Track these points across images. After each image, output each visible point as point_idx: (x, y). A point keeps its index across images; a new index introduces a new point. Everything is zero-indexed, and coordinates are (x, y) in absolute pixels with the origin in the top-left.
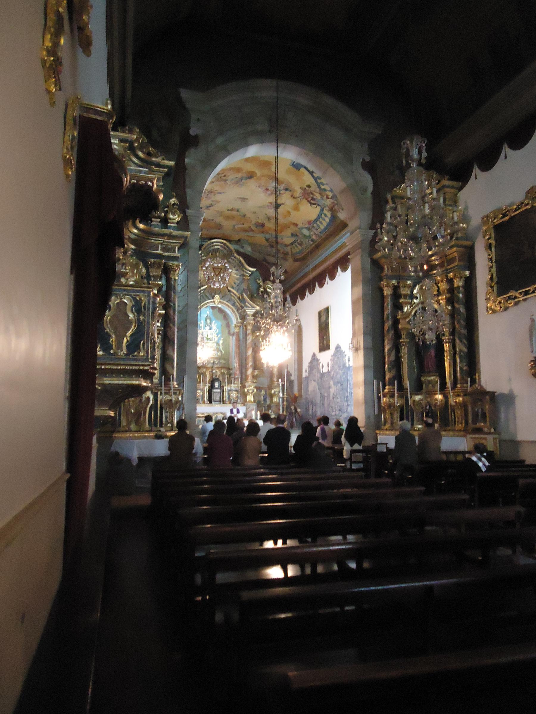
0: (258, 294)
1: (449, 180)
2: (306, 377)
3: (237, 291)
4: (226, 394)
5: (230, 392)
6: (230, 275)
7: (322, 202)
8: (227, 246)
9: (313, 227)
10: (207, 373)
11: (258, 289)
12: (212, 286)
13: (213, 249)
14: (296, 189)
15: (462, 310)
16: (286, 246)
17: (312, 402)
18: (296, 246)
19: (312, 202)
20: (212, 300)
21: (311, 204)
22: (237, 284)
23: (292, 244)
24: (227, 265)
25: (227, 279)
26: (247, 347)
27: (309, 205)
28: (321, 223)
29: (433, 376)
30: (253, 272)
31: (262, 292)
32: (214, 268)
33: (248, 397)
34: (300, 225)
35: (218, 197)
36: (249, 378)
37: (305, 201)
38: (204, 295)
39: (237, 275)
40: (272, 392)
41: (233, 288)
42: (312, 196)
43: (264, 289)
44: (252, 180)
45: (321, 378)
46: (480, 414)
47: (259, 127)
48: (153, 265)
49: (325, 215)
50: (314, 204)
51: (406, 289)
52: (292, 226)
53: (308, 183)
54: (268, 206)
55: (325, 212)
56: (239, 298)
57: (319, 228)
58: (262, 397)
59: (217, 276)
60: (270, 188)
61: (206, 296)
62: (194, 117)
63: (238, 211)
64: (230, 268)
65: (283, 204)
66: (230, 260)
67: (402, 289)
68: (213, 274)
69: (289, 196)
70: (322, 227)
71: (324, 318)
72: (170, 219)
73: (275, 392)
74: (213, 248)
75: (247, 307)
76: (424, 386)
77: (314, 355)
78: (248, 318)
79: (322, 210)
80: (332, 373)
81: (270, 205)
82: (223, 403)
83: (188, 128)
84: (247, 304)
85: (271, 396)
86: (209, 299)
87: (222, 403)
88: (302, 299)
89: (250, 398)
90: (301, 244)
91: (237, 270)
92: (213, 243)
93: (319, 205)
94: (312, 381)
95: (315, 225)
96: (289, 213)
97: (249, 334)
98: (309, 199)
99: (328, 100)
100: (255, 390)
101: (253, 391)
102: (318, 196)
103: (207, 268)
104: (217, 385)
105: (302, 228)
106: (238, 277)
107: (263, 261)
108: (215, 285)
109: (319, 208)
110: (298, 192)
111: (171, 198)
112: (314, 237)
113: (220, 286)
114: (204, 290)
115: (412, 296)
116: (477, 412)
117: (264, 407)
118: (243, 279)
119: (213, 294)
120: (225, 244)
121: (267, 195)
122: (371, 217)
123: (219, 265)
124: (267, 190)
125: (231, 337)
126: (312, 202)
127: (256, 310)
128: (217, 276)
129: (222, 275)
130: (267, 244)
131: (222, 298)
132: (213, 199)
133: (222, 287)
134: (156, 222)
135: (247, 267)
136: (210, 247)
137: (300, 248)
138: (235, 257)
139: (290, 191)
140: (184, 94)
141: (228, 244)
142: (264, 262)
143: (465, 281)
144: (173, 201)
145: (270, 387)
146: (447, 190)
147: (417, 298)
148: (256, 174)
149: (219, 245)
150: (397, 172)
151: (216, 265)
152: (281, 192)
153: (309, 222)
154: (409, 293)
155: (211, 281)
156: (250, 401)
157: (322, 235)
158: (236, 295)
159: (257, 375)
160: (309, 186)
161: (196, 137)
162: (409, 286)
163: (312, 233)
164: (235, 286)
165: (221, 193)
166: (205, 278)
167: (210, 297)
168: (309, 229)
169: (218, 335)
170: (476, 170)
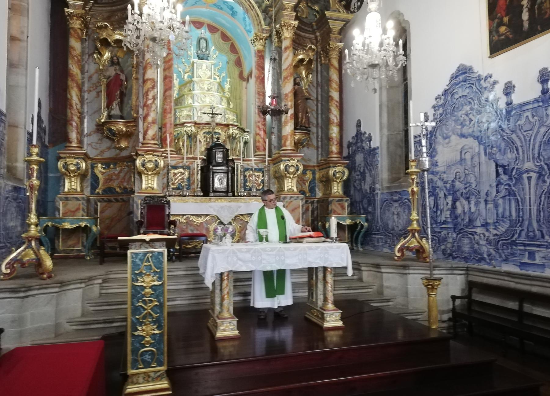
4: (240, 178)
5: (247, 174)
10: (200, 136)
17: (452, 191)
26: (284, 74)
33: (286, 181)
36: (288, 143)
58: (307, 184)
73: (334, 175)
78: (285, 12)
82: (234, 196)
85: (327, 182)
87: (230, 194)
89: (290, 184)
94: (454, 138)
97: (286, 48)
100: (301, 168)
101: (298, 170)
104: (219, 157)
117: (312, 203)
125: (244, 83)
159: (299, 140)
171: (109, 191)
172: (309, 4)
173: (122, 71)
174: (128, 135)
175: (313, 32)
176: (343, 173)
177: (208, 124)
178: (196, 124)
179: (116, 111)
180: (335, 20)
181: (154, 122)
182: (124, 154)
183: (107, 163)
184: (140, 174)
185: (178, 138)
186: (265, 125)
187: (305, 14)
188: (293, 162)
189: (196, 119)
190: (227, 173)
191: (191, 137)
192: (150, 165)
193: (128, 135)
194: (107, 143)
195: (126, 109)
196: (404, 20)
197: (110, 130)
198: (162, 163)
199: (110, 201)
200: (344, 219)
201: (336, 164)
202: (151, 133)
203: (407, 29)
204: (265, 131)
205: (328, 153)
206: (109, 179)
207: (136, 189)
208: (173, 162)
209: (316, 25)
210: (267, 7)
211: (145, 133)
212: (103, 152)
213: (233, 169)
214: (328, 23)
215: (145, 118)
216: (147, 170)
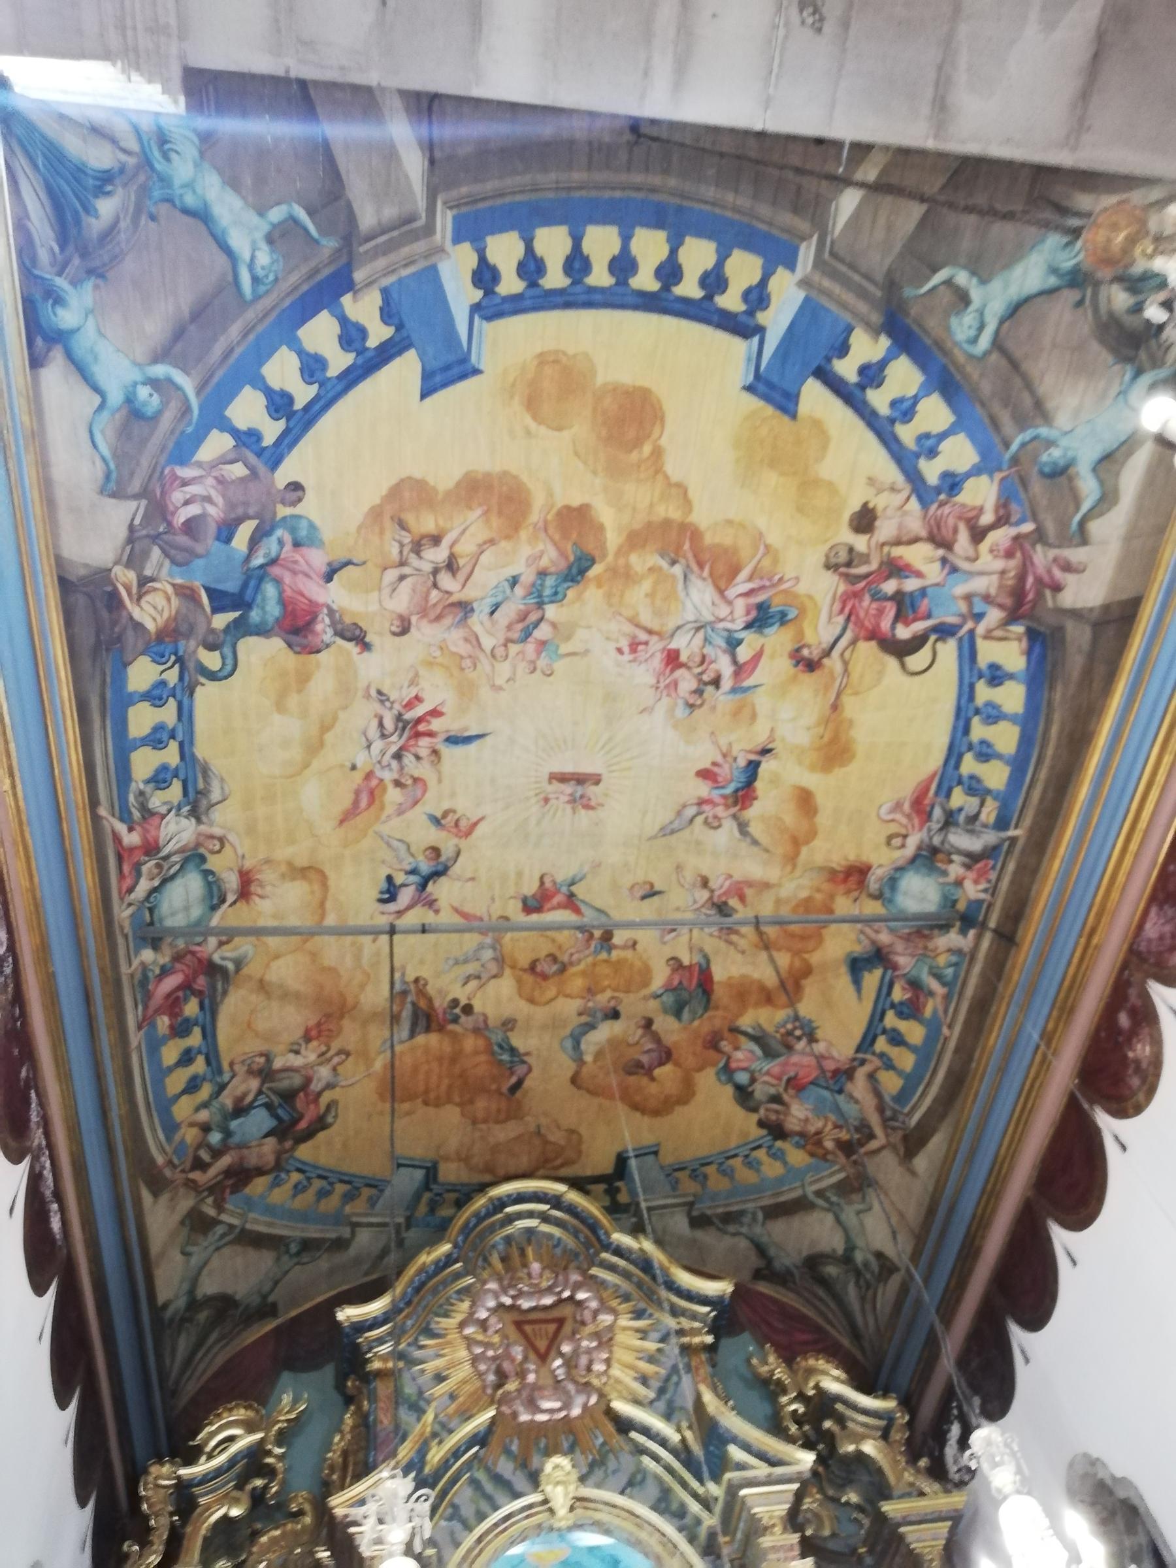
3: (668, 1416)
8: (571, 1210)
13: (508, 1240)
21: (901, 650)
22: (656, 1384)
24: (581, 1296)
31: (796, 1418)
32: (522, 1322)
34: (882, 860)
35: (459, 781)
37: (867, 649)
38: (481, 1475)
39: (643, 1334)
42: (890, 587)
43: (801, 1397)
50: (917, 643)
55: (988, 653)
59: (543, 1358)
61: (498, 1480)
63: (571, 902)
64: (604, 1307)
65: (766, 751)
66: (594, 1271)
68: (518, 1352)
74: (509, 1230)
78: (766, 1541)
81: (703, 789)
84: (736, 1453)
86: (517, 1495)
91: (638, 1314)
92: (500, 1204)
93: (944, 631)
96: (805, 801)
106: (651, 1346)
107: (758, 1275)
108: (533, 1406)
113: (567, 1406)
114: (481, 1439)
118: (685, 1349)
119: (535, 1461)
120: (556, 1202)
121: (681, 712)
123: (548, 1301)
124: (673, 659)
129: (566, 1348)
131: (593, 1468)
132: (433, 803)
133: (576, 1411)
135: (686, 1279)
136: (492, 1229)
137: (914, 1032)
138: (619, 1251)
141: (574, 1197)
142: (763, 1288)
149: (530, 1214)
151: (526, 1304)
152: (744, 654)
155: (511, 1386)
157: (1012, 833)
158: (663, 1442)
160: (864, 521)
165: (468, 740)
166: (480, 1375)
168: (930, 857)
172: (831, 1492)
180: (920, 1522)
187: (827, 1523)
196: (1113, 1478)
203: (1136, 1502)
209: (870, 1552)
210: (712, 1536)
214: (901, 1538)
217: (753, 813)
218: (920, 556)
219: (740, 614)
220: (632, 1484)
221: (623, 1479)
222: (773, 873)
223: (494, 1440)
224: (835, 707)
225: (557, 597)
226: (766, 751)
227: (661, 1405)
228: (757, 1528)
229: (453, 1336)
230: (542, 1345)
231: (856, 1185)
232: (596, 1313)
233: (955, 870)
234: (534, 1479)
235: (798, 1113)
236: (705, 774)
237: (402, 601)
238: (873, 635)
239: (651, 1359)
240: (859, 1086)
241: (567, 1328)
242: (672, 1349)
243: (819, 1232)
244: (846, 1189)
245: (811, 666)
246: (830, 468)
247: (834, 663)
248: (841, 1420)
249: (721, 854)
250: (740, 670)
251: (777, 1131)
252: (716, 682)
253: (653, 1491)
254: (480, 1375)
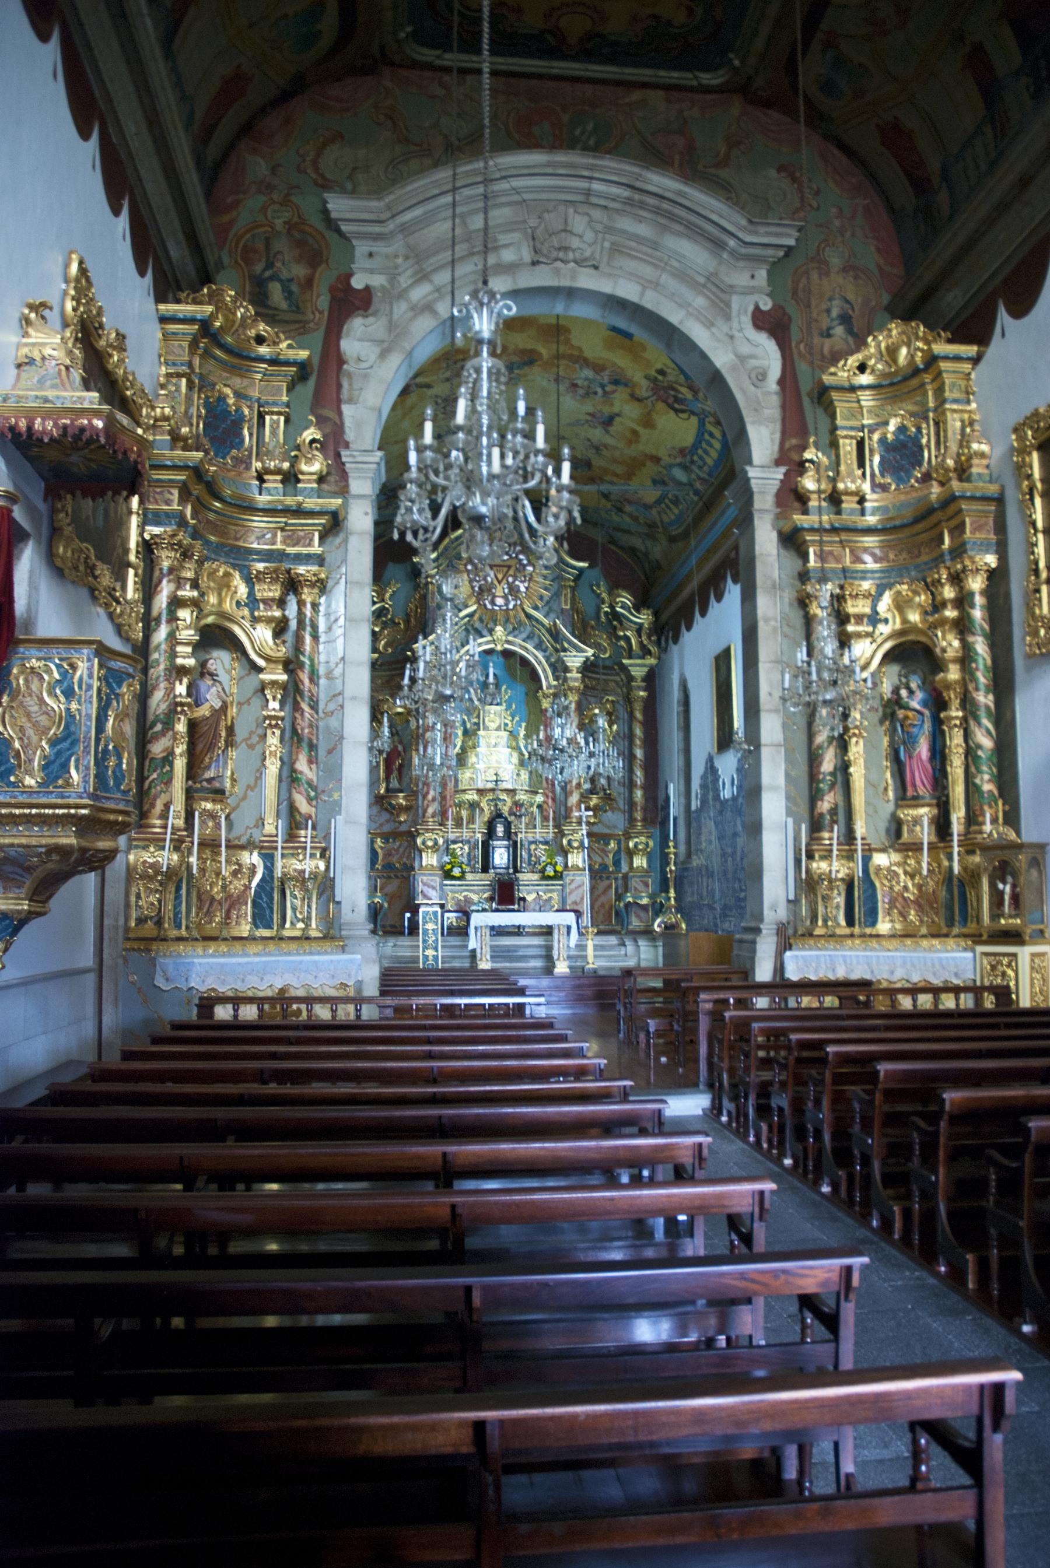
0: (598, 618)
1: (950, 341)
2: (696, 811)
6: (530, 580)
7: (698, 406)
9: (693, 462)
11: (599, 609)
12: (489, 607)
14: (636, 379)
15: (981, 647)
16: (648, 507)
18: (668, 507)
19: (676, 406)
20: (489, 638)
21: (676, 411)
22: (546, 599)
23: (659, 501)
24: (521, 557)
25: (523, 589)
27: (672, 413)
28: (706, 452)
29: (923, 806)
30: (581, 571)
31: (606, 613)
34: (666, 460)
37: (661, 405)
39: (545, 577)
40: (631, 844)
41: (536, 608)
44: (536, 369)
45: (721, 812)
46: (1007, 898)
47: (508, 256)
48: (260, 577)
49: (711, 435)
50: (683, 411)
51: (861, 602)
52: (649, 464)
53: (659, 366)
54: (587, 421)
56: (549, 631)
57: (705, 463)
58: (611, 856)
59: (500, 582)
60: (579, 382)
62: (361, 248)
65: (618, 415)
67: (850, 602)
69: (627, 397)
70: (709, 461)
71: (723, 669)
72: (303, 473)
73: (636, 845)
75: (565, 650)
76: (905, 828)
77: (710, 759)
79: (702, 423)
80: (740, 800)
81: (589, 418)
83: (350, 275)
85: (631, 854)
86: (482, 636)
88: (689, 628)
90: (676, 502)
93: (693, 413)
95: (695, 458)
96: (635, 433)
98: (671, 400)
99: (661, 181)
101: (582, 843)
102: (685, 392)
103: (530, 563)
104: (500, 830)
105: (671, 466)
108: (493, 603)
109: (694, 420)
110: (644, 388)
111: (307, 428)
112: (698, 485)
113: (507, 604)
114: (471, 615)
115: (874, 619)
116: (1002, 893)
117: (616, 879)
122: (777, 436)
124: (575, 385)
126: (676, 406)
127: (588, 659)
128: (500, 582)
130: (609, 505)
133: (511, 606)
134: (275, 481)
137: (676, 511)
139: (626, 385)
140: (338, 205)
142: (613, 547)
143: (989, 579)
144: (310, 434)
145: (628, 837)
146: (943, 365)
147: (886, 621)
148: (540, 354)
150: (839, 330)
152: (608, 389)
153: (682, 452)
154: (867, 610)
156: (577, 868)
158: (543, 625)
160: (661, 372)
161: (367, 289)
162: (867, 595)
163: (693, 476)
164: (539, 604)
167: (485, 632)
168: (685, 468)
169: (513, 716)
170: (1003, 316)
171: (388, 867)
173: (401, 742)
174: (407, 809)
175: (618, 674)
176: (647, 845)
177: (493, 790)
178: (481, 792)
179: (394, 784)
181: (434, 800)
182: (403, 828)
183: (386, 837)
184: (420, 851)
185: (459, 805)
186: (553, 792)
188: (577, 836)
189: (480, 785)
190: (508, 848)
191: (473, 806)
192: (430, 843)
193: (407, 809)
194: (386, 816)
195: (406, 780)
197: (390, 804)
198: (441, 841)
199: (389, 877)
200: (641, 898)
201: (641, 834)
202: (430, 811)
204: (554, 800)
205: (632, 820)
206: (388, 854)
207: (416, 865)
208: (452, 836)
211: (425, 811)
212: (381, 825)
213: (515, 843)
215: (425, 797)
216: (427, 847)
217: (611, 429)
218: (684, 390)
219: (606, 380)
220: (528, 638)
221: (524, 636)
222: (621, 445)
223: (476, 617)
224: (649, 413)
225: (519, 368)
226: (618, 415)
227: (546, 609)
228: (566, 669)
229: (462, 567)
230: (500, 577)
231: (651, 536)
232: (524, 566)
233: (693, 476)
234: (491, 631)
235: (628, 508)
236: (589, 414)
237: (448, 374)
238: (665, 401)
239: (546, 589)
240: (654, 511)
241: (511, 572)
242: (556, 585)
243: (638, 543)
244: (647, 535)
245: (639, 400)
246: (646, 355)
247: (649, 402)
248: (621, 623)
249: (597, 434)
250: (605, 393)
251: (620, 510)
252: (596, 393)
253: (536, 640)
254: (473, 588)
